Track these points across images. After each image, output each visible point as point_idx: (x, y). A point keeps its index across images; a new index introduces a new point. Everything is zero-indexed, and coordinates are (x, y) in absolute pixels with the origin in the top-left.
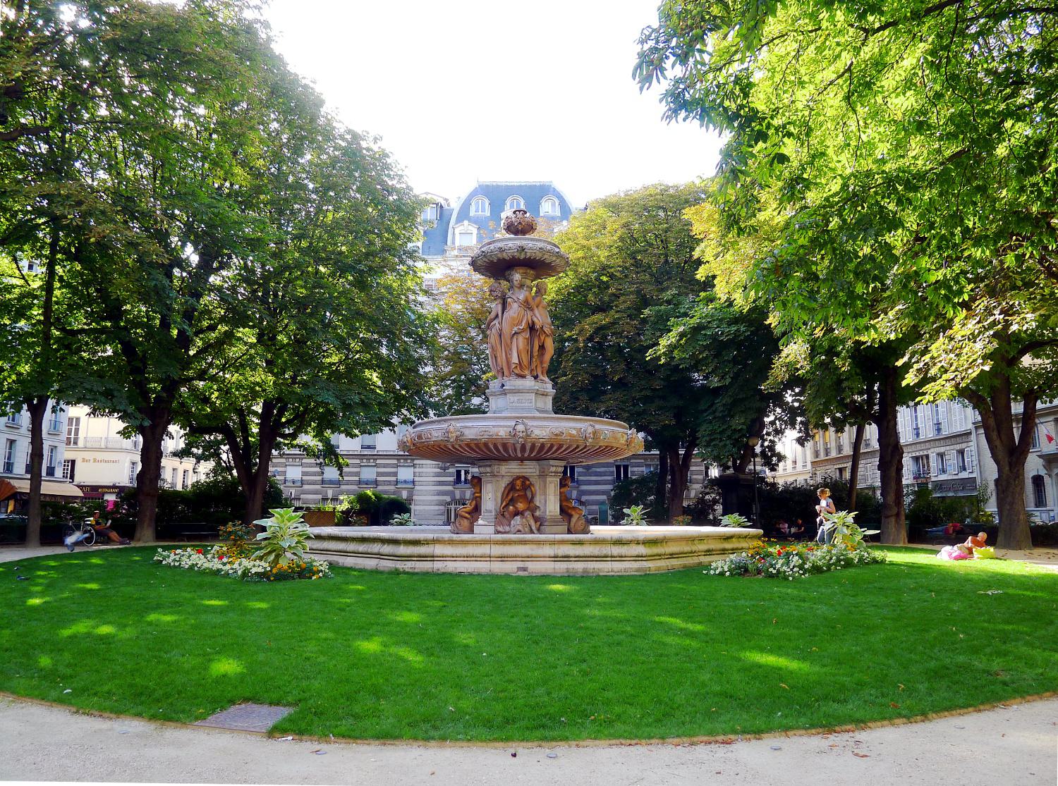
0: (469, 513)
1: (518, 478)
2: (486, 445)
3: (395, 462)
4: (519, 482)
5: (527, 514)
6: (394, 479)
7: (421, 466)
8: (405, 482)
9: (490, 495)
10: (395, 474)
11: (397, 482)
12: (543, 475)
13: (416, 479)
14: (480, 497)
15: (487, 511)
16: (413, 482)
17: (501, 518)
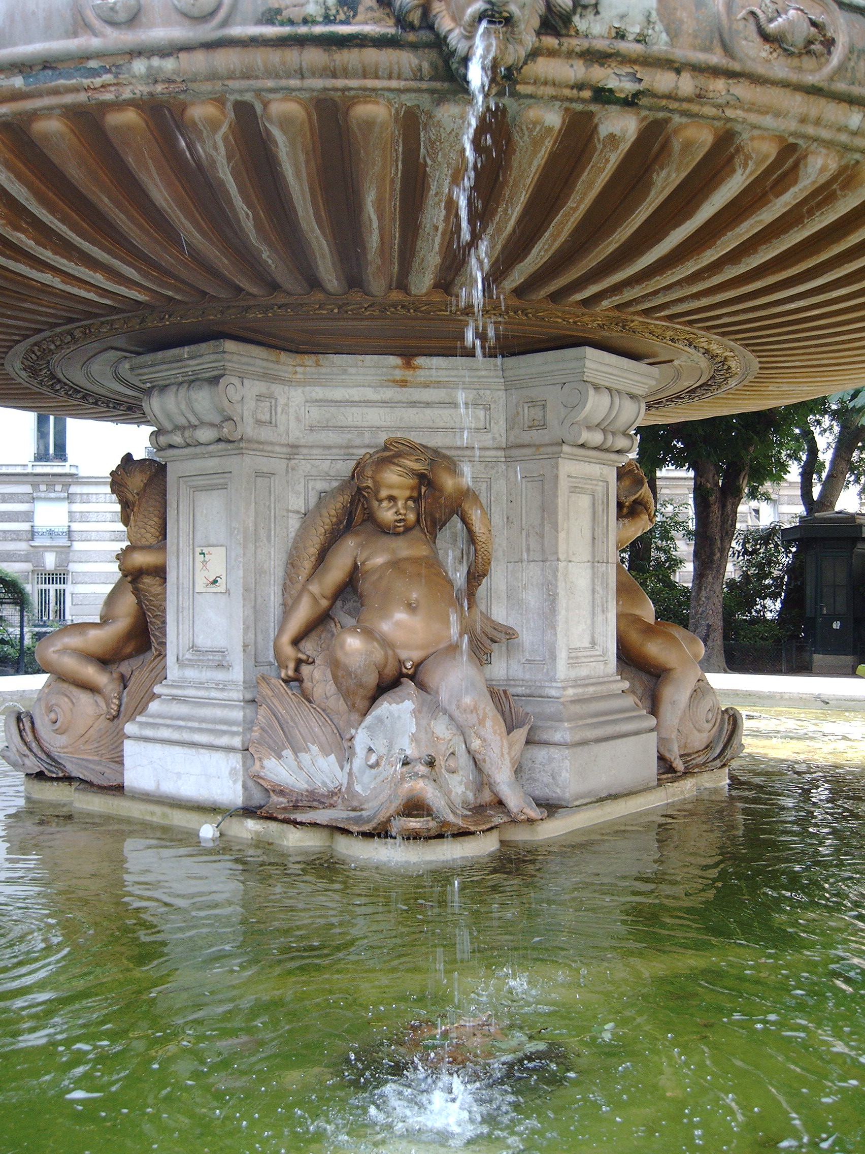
0: (104, 661)
1: (391, 453)
2: (164, 115)
3: (27, 489)
4: (395, 480)
5: (457, 680)
6: (25, 526)
7: (86, 498)
8: (51, 533)
9: (217, 563)
10: (28, 516)
11: (33, 534)
12: (534, 446)
13: (75, 526)
14: (160, 572)
15: (201, 656)
16: (69, 533)
17: (286, 702)
